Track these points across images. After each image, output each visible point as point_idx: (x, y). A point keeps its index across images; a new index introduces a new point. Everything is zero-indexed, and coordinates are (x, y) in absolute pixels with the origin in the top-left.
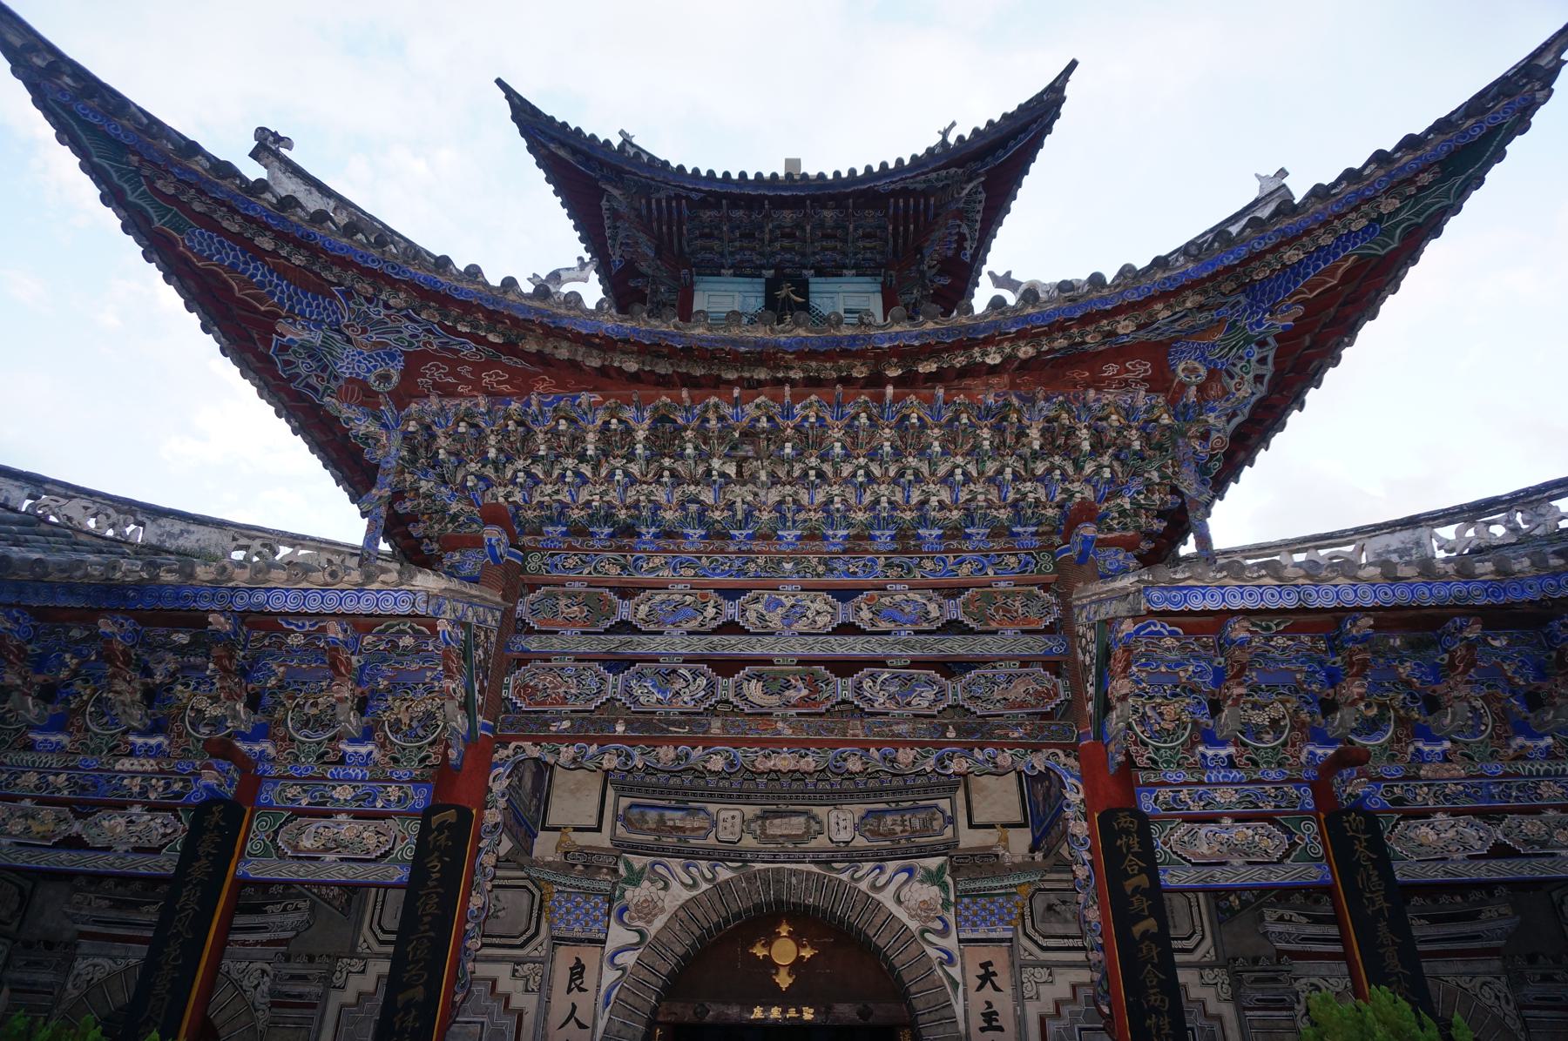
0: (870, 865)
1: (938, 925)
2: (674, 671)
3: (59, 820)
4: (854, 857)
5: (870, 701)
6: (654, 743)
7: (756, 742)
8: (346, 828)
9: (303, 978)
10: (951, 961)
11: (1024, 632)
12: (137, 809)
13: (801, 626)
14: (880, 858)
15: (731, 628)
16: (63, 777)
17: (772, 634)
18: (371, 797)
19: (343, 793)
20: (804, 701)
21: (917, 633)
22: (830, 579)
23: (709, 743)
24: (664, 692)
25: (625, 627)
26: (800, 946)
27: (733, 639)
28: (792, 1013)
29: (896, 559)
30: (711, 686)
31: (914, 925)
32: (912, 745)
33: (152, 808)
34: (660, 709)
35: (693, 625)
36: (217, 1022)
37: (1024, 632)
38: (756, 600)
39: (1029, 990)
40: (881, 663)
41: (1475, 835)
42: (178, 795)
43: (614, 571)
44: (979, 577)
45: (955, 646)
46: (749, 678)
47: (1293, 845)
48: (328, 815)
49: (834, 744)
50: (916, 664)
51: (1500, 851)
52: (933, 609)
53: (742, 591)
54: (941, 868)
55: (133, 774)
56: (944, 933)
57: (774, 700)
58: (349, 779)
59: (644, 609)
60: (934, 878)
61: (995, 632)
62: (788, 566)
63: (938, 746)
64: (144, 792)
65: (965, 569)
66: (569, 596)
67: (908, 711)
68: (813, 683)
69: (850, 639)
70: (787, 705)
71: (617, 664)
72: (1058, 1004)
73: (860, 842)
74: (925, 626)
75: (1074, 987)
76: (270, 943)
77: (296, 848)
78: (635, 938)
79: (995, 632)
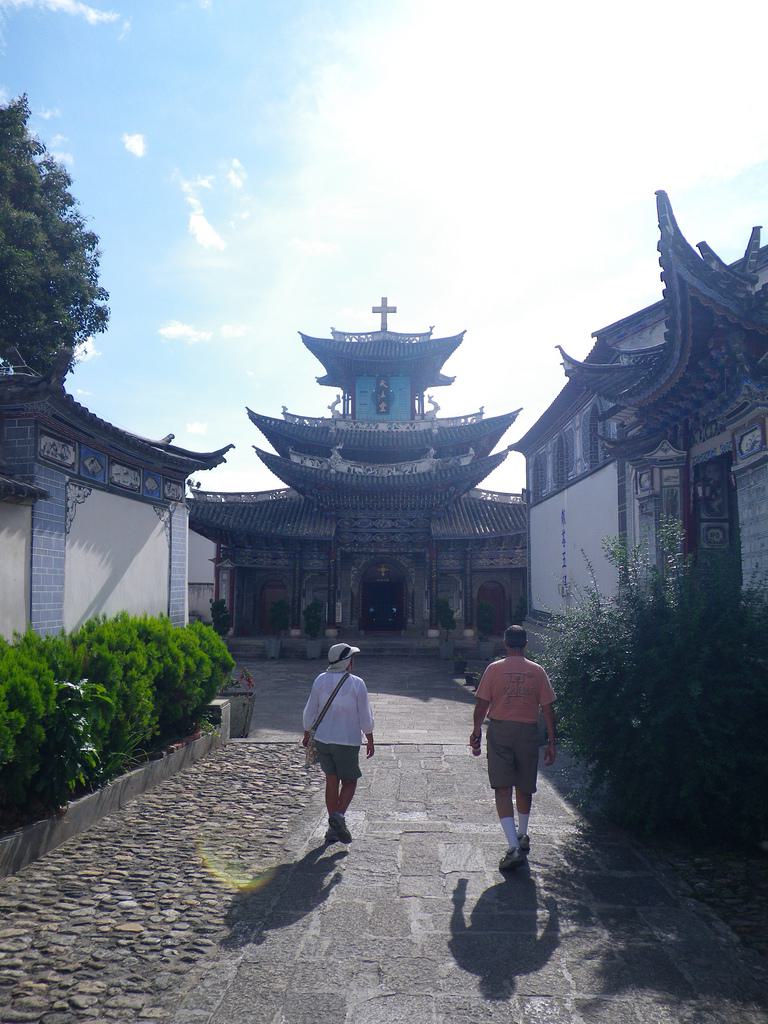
8: (317, 562)
25: (356, 527)
45: (411, 531)
71: (356, 533)
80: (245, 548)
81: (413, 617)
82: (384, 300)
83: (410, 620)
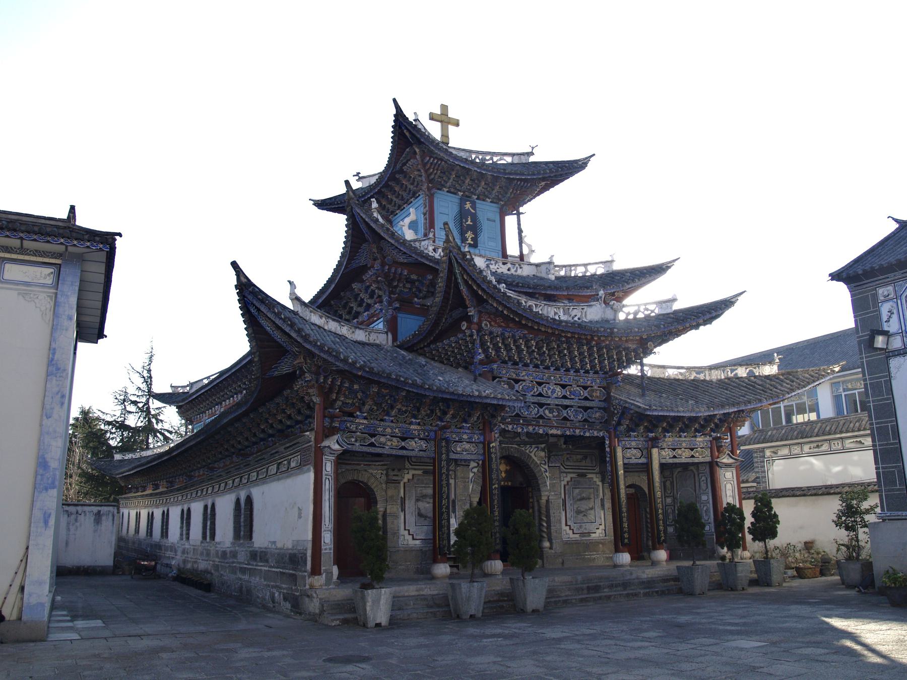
0: (528, 446)
1: (544, 462)
2: (530, 406)
3: (398, 442)
4: (525, 443)
5: (570, 417)
6: (528, 425)
7: (548, 426)
8: (467, 446)
9: (397, 475)
10: (546, 471)
11: (600, 401)
12: (417, 439)
13: (555, 395)
14: (531, 444)
15: (540, 395)
16: (397, 430)
17: (549, 397)
18: (471, 438)
19: (465, 437)
20: (557, 416)
21: (579, 399)
22: (561, 383)
23: (539, 426)
24: (528, 411)
26: (507, 466)
27: (543, 398)
28: (506, 484)
29: (575, 378)
30: (538, 410)
31: (538, 462)
32: (579, 428)
33: (421, 439)
34: (528, 416)
35: (532, 393)
36: (372, 487)
37: (600, 401)
38: (545, 387)
39: (562, 478)
40: (572, 406)
41: (671, 453)
42: (428, 436)
43: (514, 376)
44: (591, 385)
46: (545, 409)
47: (642, 454)
48: (461, 442)
49: (564, 428)
50: (579, 407)
51: (675, 457)
52: (581, 392)
53: (542, 383)
54: (544, 447)
55: (415, 430)
56: (545, 464)
57: (551, 415)
58: (466, 433)
59: (521, 387)
60: (543, 450)
61: (593, 400)
62: (552, 378)
63: (583, 429)
64: (419, 435)
65: (589, 382)
66: (504, 381)
67: (577, 420)
68: (558, 411)
69: (567, 400)
70: (554, 417)
72: (568, 482)
73: (527, 439)
74: (580, 398)
75: (571, 478)
76: (382, 465)
77: (456, 450)
78: (476, 465)
79: (593, 400)
80: (357, 417)
81: (550, 540)
82: (444, 108)
83: (546, 544)
